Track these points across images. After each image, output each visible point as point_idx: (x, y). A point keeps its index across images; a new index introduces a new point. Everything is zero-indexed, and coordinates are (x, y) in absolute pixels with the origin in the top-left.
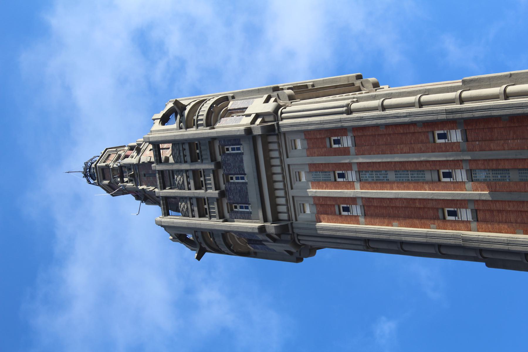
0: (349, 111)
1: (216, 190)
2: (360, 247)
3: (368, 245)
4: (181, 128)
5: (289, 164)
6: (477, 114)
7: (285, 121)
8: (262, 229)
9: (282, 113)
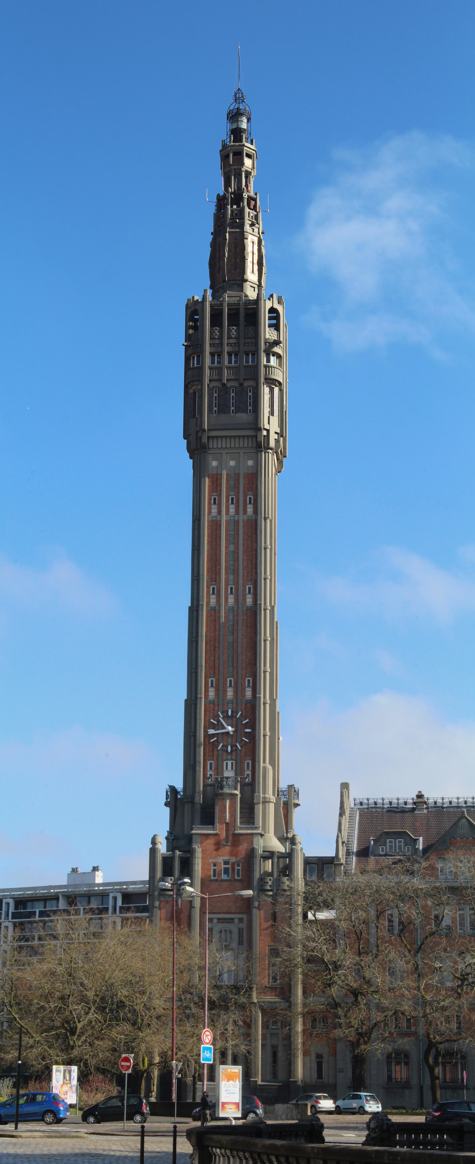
0: (265, 519)
1: (227, 380)
2: (195, 513)
4: (265, 343)
6: (258, 617)
7: (263, 455)
8: (204, 430)
9: (268, 453)
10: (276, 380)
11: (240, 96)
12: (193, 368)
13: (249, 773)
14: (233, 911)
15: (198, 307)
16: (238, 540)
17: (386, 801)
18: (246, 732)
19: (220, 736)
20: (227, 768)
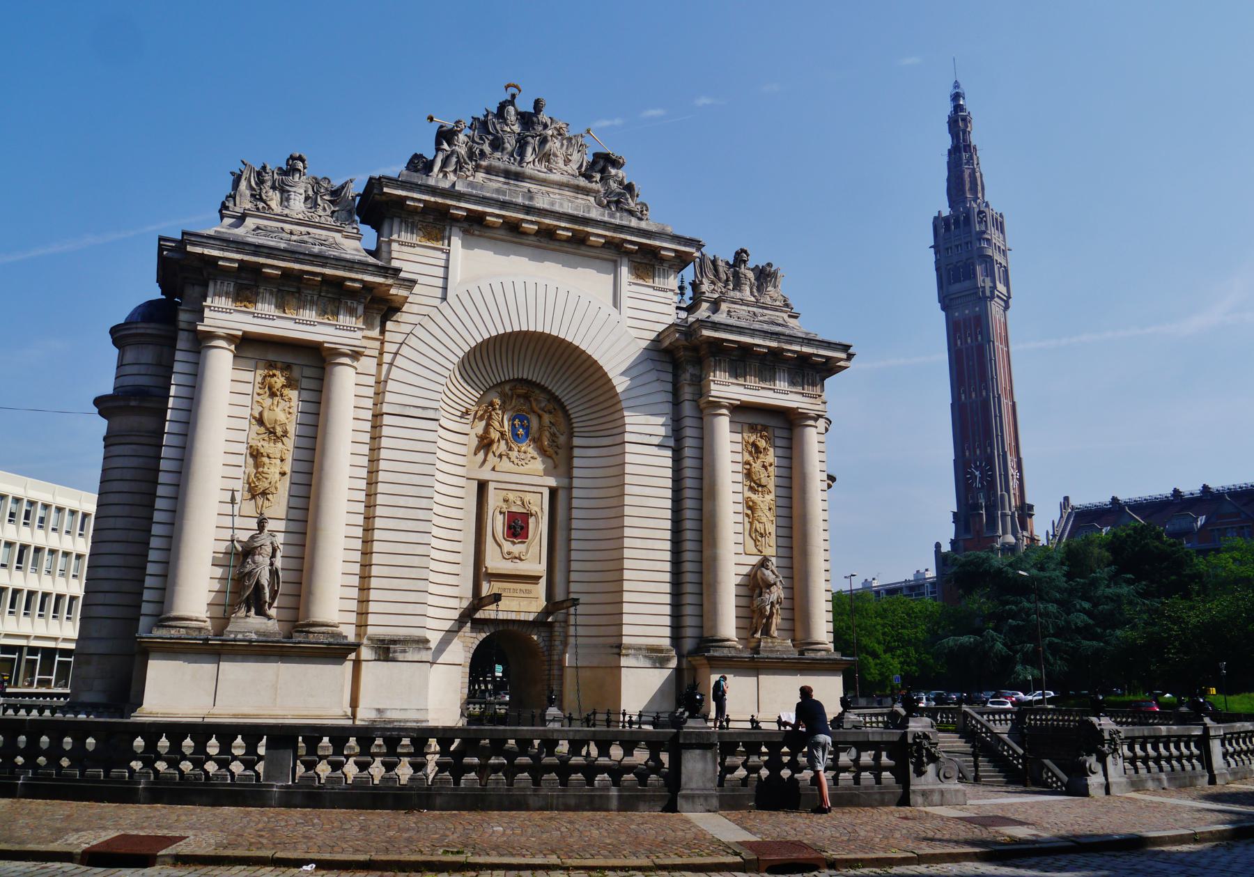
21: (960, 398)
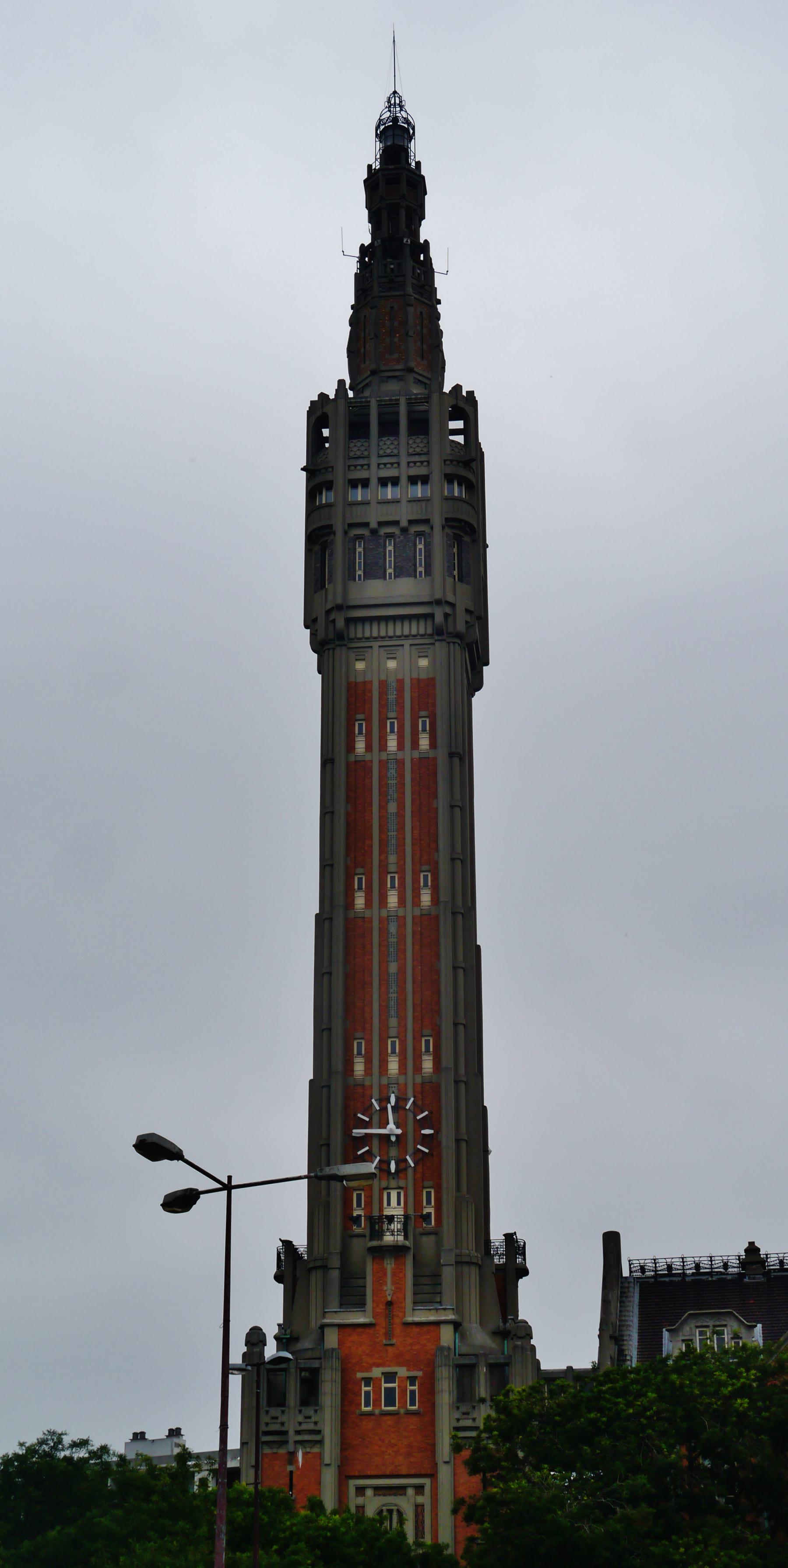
3: (328, 761)
5: (405, 646)
9: (454, 643)
10: (466, 522)
11: (397, 101)
12: (322, 506)
13: (431, 1210)
14: (404, 1472)
15: (329, 409)
16: (404, 794)
17: (689, 1264)
18: (424, 1135)
19: (375, 1143)
20: (389, 1204)
21: (349, 904)
